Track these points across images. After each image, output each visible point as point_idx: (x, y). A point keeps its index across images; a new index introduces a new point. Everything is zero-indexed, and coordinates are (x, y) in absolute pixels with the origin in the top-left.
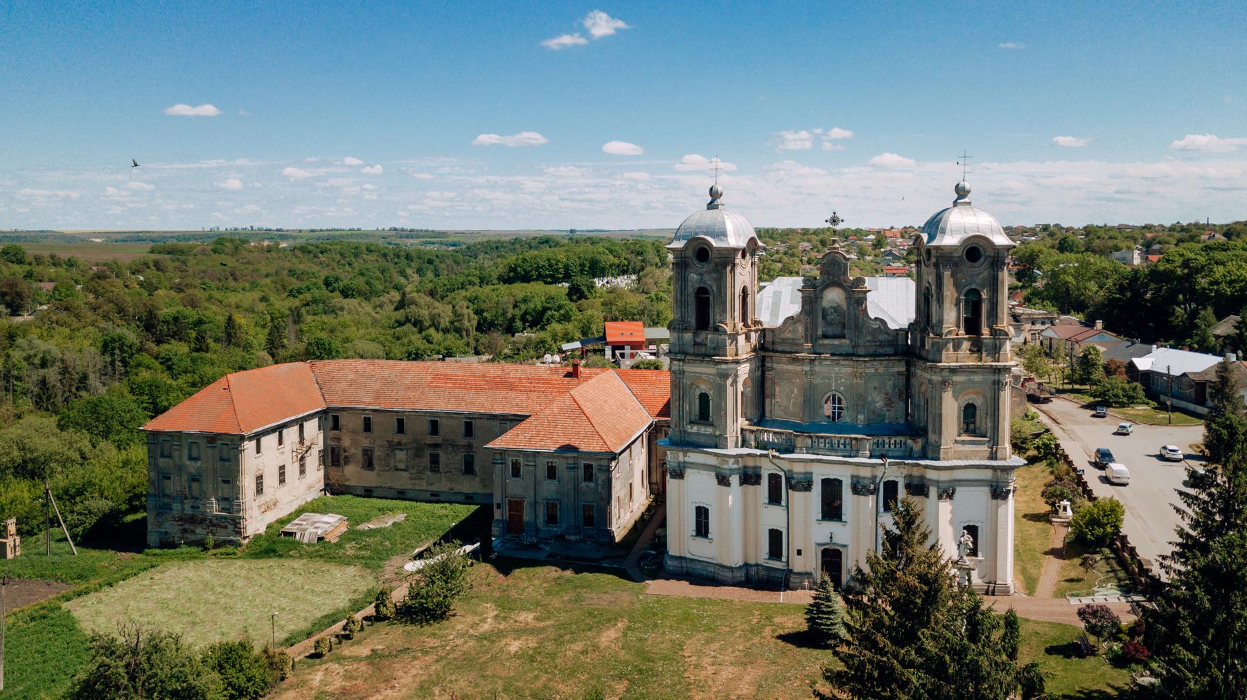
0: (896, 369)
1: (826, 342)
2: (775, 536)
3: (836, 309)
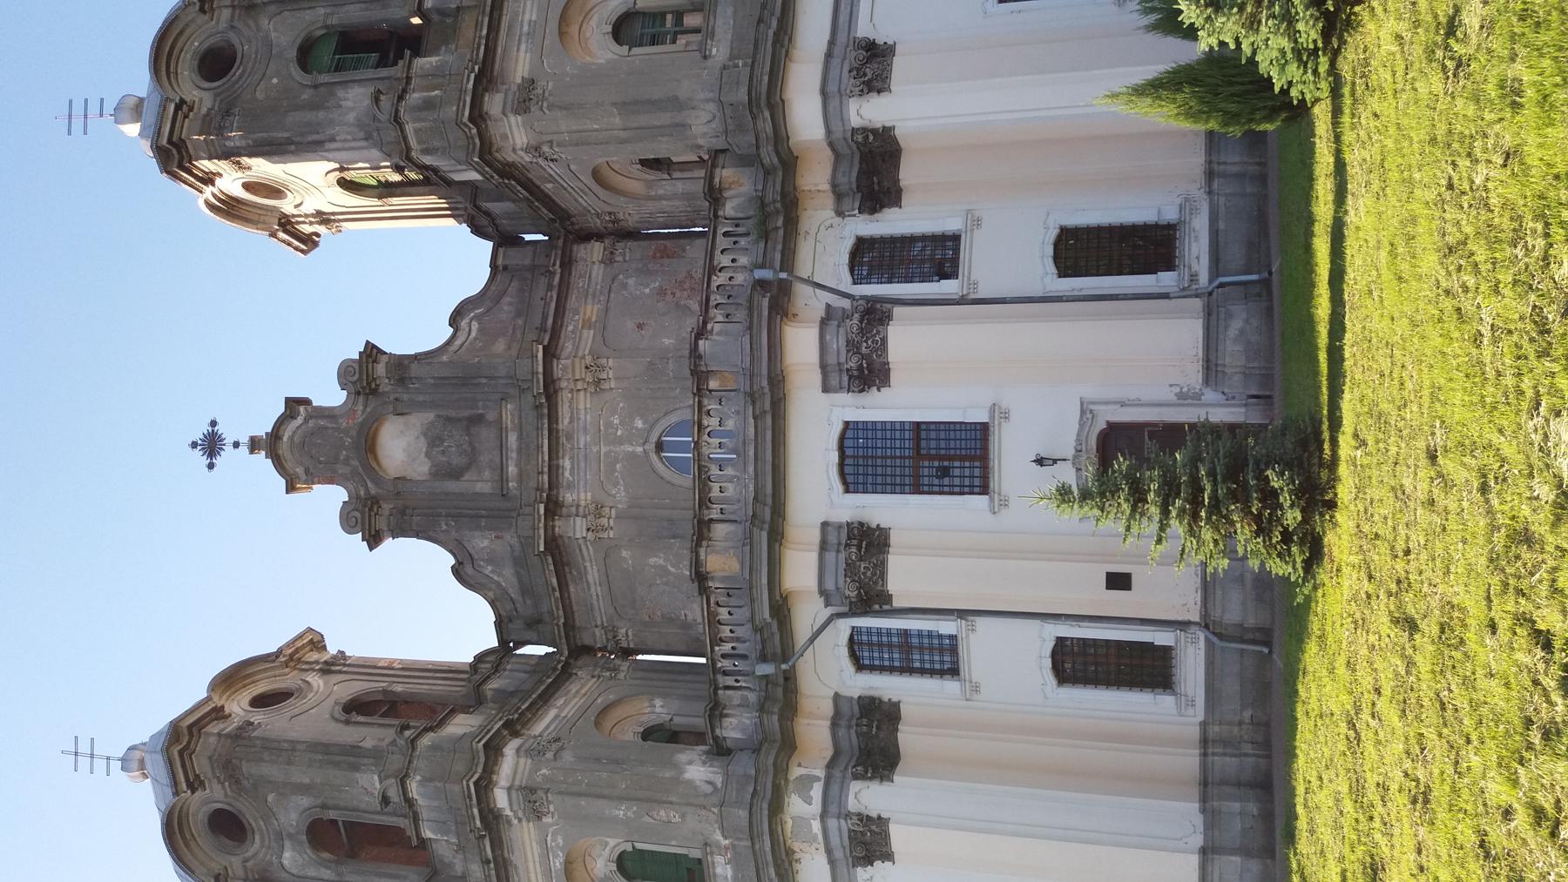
0: (598, 272)
1: (512, 469)
2: (1077, 663)
3: (434, 440)
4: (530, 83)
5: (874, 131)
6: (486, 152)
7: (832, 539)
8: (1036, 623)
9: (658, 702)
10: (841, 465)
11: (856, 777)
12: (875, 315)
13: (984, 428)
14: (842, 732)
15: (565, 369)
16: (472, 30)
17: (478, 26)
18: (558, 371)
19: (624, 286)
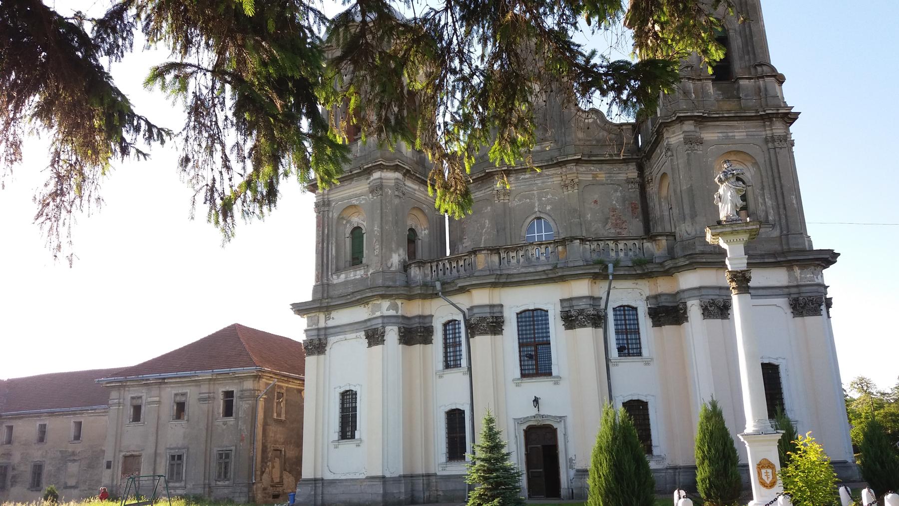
0: (622, 177)
4: (701, 142)
5: (685, 312)
6: (666, 125)
7: (496, 310)
8: (469, 402)
9: (426, 232)
10: (529, 310)
11: (399, 328)
12: (598, 320)
13: (550, 374)
14: (417, 320)
15: (571, 169)
16: (729, 106)
17: (729, 111)
18: (569, 166)
19: (616, 191)
